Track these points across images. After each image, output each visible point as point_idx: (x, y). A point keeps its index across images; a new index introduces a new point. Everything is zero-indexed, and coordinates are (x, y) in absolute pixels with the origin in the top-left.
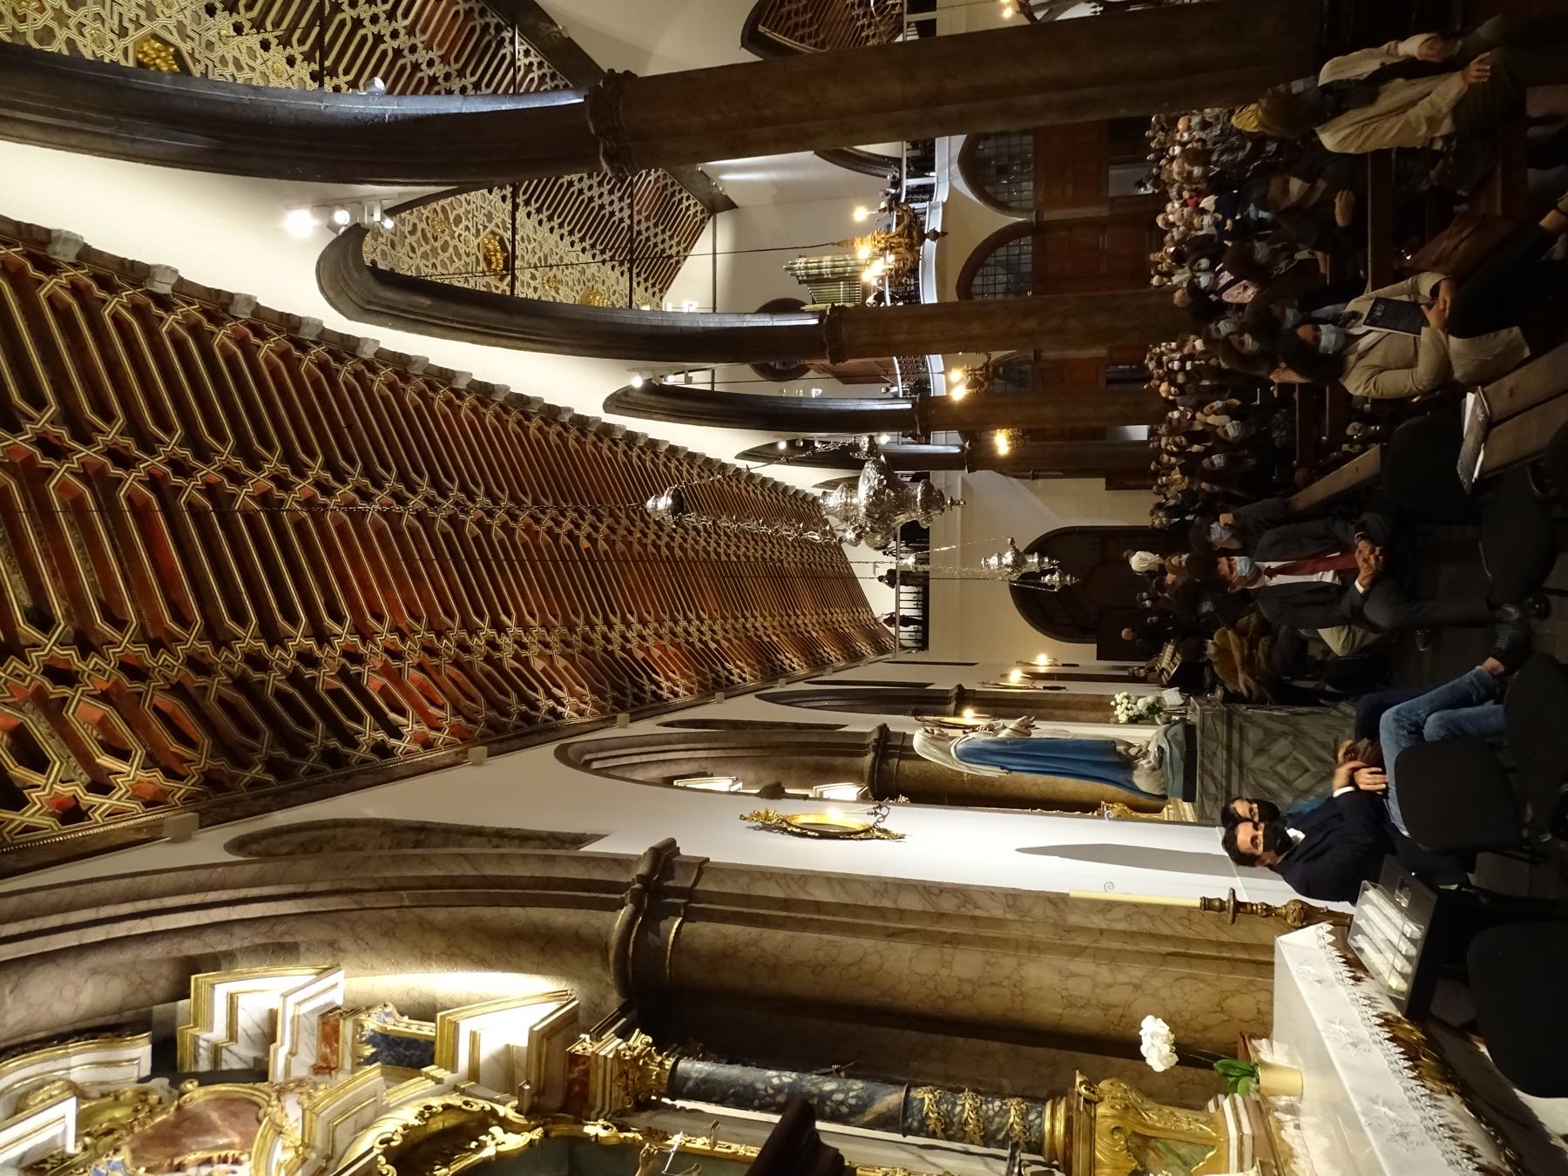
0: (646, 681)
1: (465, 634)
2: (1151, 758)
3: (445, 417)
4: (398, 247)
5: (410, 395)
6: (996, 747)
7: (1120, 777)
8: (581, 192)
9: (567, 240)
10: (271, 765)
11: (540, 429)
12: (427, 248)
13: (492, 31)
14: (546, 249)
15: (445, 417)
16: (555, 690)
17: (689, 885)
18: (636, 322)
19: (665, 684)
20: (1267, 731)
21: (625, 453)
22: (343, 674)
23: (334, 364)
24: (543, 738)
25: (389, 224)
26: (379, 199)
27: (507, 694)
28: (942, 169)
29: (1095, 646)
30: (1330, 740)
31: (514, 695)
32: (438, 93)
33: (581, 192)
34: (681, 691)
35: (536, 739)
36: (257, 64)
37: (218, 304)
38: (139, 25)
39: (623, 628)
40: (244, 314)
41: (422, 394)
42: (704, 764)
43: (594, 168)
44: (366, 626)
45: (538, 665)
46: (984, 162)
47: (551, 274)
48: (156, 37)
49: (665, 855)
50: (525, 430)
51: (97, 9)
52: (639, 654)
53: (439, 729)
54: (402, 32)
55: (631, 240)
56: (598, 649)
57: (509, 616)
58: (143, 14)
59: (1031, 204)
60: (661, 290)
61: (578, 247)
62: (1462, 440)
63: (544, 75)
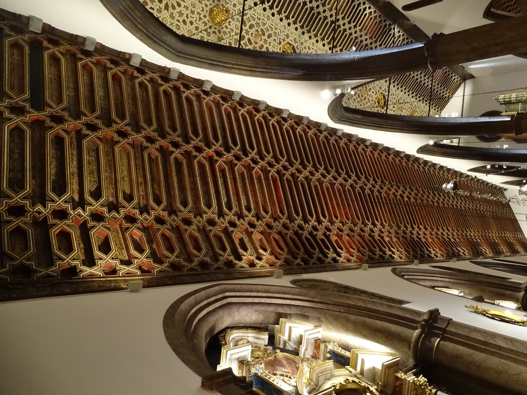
0: (425, 250)
1: (363, 226)
3: (362, 154)
4: (350, 100)
5: (351, 147)
9: (407, 94)
10: (303, 260)
11: (393, 159)
12: (359, 99)
13: (388, 26)
14: (399, 98)
15: (362, 154)
16: (392, 249)
17: (444, 327)
19: (433, 252)
21: (423, 168)
22: (325, 234)
24: (387, 264)
25: (353, 92)
27: (375, 248)
31: (378, 249)
34: (439, 255)
35: (385, 264)
36: (315, 48)
37: (299, 120)
38: (284, 40)
39: (418, 230)
40: (305, 122)
41: (355, 147)
42: (448, 284)
44: (332, 220)
47: (400, 106)
48: (288, 43)
49: (434, 314)
50: (388, 159)
51: (274, 38)
52: (424, 240)
53: (353, 256)
54: (358, 31)
55: (431, 92)
56: (408, 236)
57: (378, 221)
58: (285, 37)
60: (441, 110)
61: (411, 96)
63: (404, 38)
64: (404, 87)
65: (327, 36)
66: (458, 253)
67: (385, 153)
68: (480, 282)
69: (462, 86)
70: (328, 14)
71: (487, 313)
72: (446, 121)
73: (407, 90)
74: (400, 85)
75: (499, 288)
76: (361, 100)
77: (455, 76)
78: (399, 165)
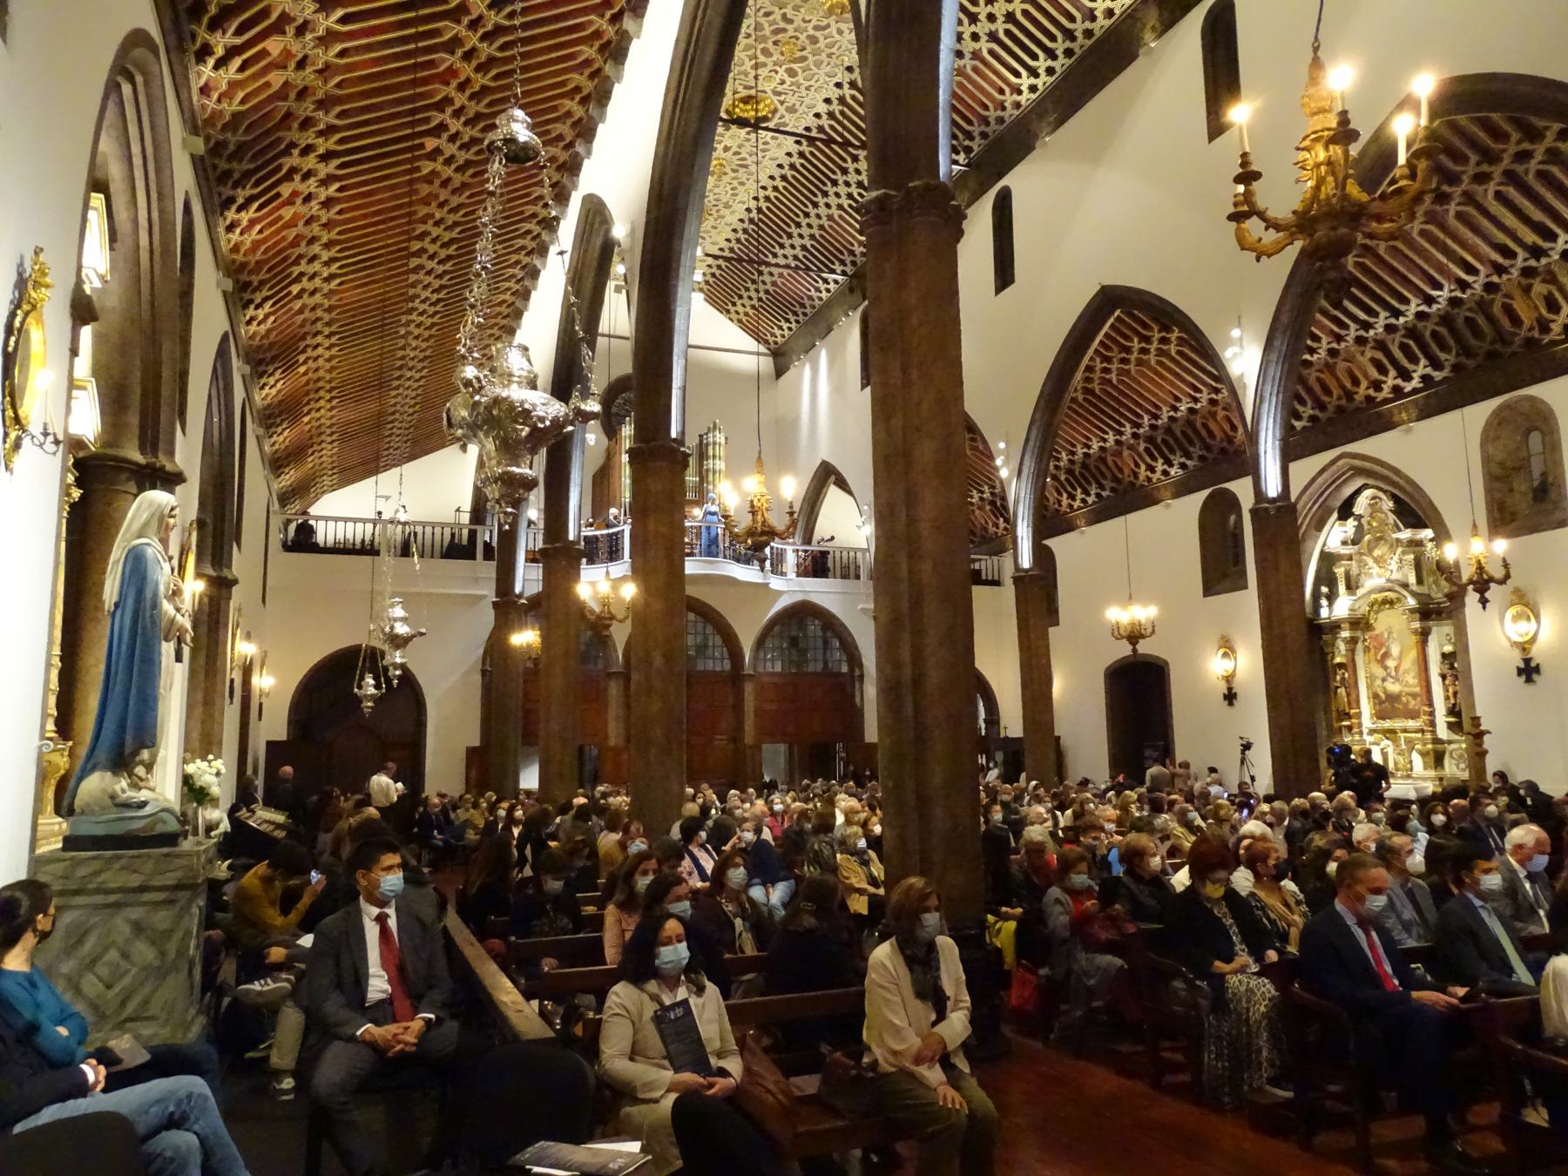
0: (249, 192)
2: (131, 793)
6: (148, 594)
7: (102, 755)
8: (807, 215)
11: (569, 114)
12: (767, 31)
13: (967, 143)
16: (237, 62)
19: (245, 217)
20: (169, 933)
21: (534, 215)
24: (168, 24)
28: (799, 584)
29: (284, 738)
30: (154, 1009)
32: (960, 23)
33: (807, 215)
34: (235, 237)
35: (168, 16)
39: (322, 175)
42: (129, 241)
43: (876, 181)
45: (274, 45)
46: (802, 626)
47: (728, 170)
50: (570, 94)
52: (285, 190)
54: (977, 46)
55: (751, 261)
59: (761, 669)
66: (251, 301)
67: (589, 87)
68: (153, 340)
69: (762, 349)
71: (27, 314)
72: (681, 275)
73: (772, 194)
75: (144, 396)
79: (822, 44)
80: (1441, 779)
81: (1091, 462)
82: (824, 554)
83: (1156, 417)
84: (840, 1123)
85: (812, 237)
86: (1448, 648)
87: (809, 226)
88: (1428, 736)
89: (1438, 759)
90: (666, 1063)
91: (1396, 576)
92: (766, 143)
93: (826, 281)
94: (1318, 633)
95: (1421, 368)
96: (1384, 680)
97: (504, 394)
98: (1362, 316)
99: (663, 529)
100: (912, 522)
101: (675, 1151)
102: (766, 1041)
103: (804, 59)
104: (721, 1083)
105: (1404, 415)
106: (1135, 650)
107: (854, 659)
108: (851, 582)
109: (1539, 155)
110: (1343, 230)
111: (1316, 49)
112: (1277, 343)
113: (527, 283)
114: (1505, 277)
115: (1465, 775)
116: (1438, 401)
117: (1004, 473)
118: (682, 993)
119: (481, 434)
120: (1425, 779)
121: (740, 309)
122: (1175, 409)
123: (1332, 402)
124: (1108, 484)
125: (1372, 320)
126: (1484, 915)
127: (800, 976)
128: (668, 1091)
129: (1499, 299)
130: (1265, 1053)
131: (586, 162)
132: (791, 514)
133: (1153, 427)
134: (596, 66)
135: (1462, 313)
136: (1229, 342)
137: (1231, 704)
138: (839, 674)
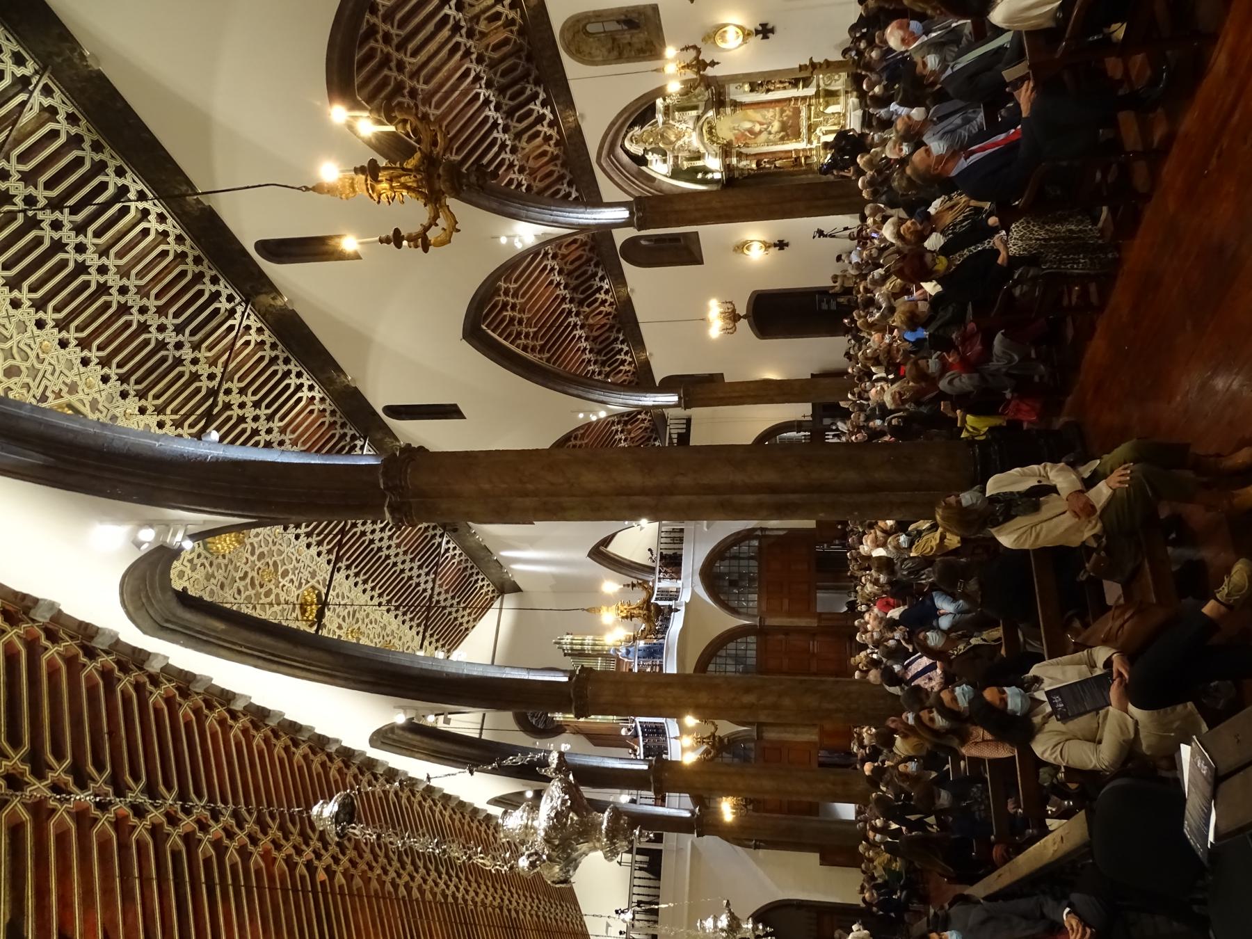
4: (227, 589)
8: (395, 564)
11: (305, 757)
12: (251, 592)
13: (348, 439)
18: (407, 664)
23: (117, 673)
25: (188, 545)
26: (185, 523)
28: (686, 578)
33: (395, 564)
38: (58, 395)
40: (42, 617)
41: (197, 711)
46: (720, 576)
47: (356, 627)
51: (29, 380)
54: (276, 430)
58: (65, 389)
62: (1184, 800)
64: (370, 585)
65: (193, 417)
69: (497, 604)
70: (203, 369)
74: (362, 577)
76: (258, 595)
77: (483, 580)
78: (318, 775)
79: (265, 549)
80: (847, 92)
81: (598, 347)
82: (663, 557)
83: (564, 299)
84: (1147, 565)
85: (412, 560)
86: (747, 87)
87: (403, 562)
88: (813, 101)
89: (831, 95)
90: (1102, 712)
91: (691, 125)
92: (338, 596)
93: (447, 550)
94: (732, 180)
95: (537, 107)
96: (770, 133)
97: (543, 834)
98: (496, 149)
99: (643, 690)
100: (644, 492)
101: (1179, 708)
102: (1077, 624)
103: (275, 563)
104: (1117, 665)
105: (571, 119)
106: (745, 317)
107: (747, 535)
108: (685, 535)
109: (387, 27)
110: (441, 171)
111: (307, 189)
112: (513, 210)
113: (436, 797)
114: (473, 50)
115: (844, 75)
116: (560, 93)
117: (603, 414)
118: (1040, 695)
119: (575, 855)
120: (846, 104)
121: (466, 619)
122: (559, 284)
123: (558, 170)
124: (613, 336)
125: (499, 142)
126: (958, 67)
127: (1025, 600)
128: (1126, 711)
129: (489, 54)
130: (1073, 227)
131: (344, 744)
132: (633, 585)
133: (571, 302)
134: (270, 733)
135: (498, 80)
136: (511, 245)
137: (787, 245)
138: (760, 547)
